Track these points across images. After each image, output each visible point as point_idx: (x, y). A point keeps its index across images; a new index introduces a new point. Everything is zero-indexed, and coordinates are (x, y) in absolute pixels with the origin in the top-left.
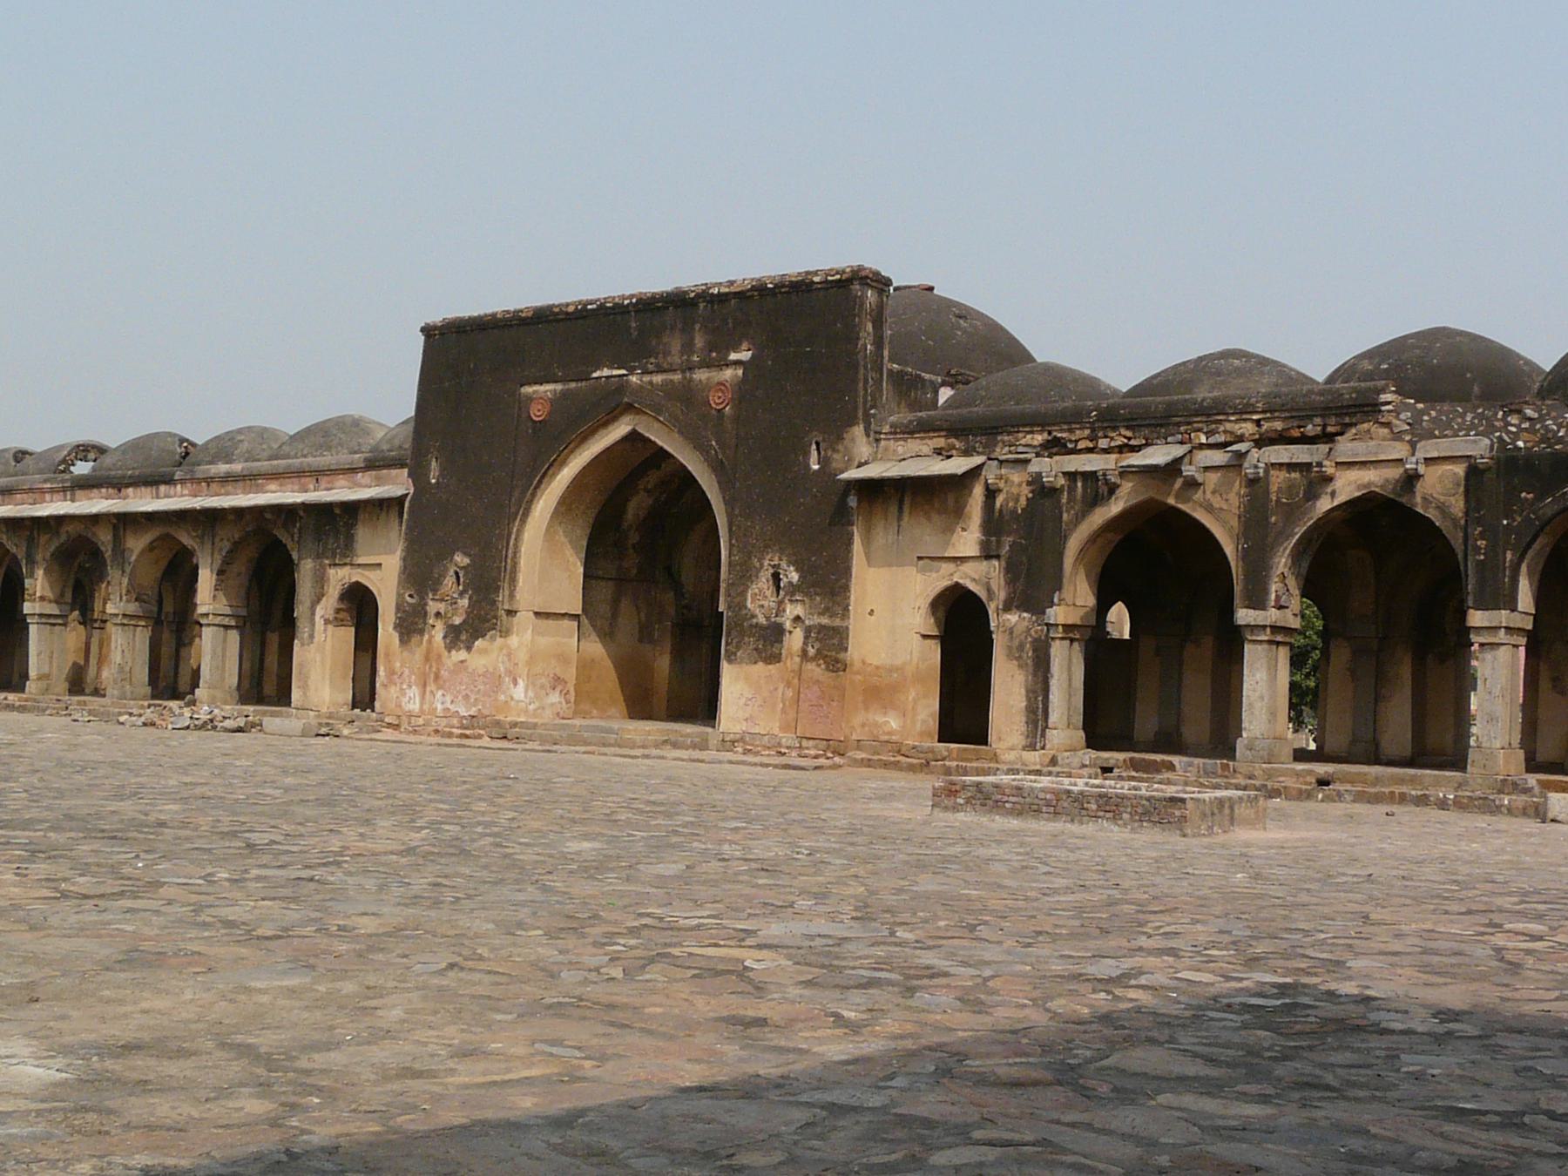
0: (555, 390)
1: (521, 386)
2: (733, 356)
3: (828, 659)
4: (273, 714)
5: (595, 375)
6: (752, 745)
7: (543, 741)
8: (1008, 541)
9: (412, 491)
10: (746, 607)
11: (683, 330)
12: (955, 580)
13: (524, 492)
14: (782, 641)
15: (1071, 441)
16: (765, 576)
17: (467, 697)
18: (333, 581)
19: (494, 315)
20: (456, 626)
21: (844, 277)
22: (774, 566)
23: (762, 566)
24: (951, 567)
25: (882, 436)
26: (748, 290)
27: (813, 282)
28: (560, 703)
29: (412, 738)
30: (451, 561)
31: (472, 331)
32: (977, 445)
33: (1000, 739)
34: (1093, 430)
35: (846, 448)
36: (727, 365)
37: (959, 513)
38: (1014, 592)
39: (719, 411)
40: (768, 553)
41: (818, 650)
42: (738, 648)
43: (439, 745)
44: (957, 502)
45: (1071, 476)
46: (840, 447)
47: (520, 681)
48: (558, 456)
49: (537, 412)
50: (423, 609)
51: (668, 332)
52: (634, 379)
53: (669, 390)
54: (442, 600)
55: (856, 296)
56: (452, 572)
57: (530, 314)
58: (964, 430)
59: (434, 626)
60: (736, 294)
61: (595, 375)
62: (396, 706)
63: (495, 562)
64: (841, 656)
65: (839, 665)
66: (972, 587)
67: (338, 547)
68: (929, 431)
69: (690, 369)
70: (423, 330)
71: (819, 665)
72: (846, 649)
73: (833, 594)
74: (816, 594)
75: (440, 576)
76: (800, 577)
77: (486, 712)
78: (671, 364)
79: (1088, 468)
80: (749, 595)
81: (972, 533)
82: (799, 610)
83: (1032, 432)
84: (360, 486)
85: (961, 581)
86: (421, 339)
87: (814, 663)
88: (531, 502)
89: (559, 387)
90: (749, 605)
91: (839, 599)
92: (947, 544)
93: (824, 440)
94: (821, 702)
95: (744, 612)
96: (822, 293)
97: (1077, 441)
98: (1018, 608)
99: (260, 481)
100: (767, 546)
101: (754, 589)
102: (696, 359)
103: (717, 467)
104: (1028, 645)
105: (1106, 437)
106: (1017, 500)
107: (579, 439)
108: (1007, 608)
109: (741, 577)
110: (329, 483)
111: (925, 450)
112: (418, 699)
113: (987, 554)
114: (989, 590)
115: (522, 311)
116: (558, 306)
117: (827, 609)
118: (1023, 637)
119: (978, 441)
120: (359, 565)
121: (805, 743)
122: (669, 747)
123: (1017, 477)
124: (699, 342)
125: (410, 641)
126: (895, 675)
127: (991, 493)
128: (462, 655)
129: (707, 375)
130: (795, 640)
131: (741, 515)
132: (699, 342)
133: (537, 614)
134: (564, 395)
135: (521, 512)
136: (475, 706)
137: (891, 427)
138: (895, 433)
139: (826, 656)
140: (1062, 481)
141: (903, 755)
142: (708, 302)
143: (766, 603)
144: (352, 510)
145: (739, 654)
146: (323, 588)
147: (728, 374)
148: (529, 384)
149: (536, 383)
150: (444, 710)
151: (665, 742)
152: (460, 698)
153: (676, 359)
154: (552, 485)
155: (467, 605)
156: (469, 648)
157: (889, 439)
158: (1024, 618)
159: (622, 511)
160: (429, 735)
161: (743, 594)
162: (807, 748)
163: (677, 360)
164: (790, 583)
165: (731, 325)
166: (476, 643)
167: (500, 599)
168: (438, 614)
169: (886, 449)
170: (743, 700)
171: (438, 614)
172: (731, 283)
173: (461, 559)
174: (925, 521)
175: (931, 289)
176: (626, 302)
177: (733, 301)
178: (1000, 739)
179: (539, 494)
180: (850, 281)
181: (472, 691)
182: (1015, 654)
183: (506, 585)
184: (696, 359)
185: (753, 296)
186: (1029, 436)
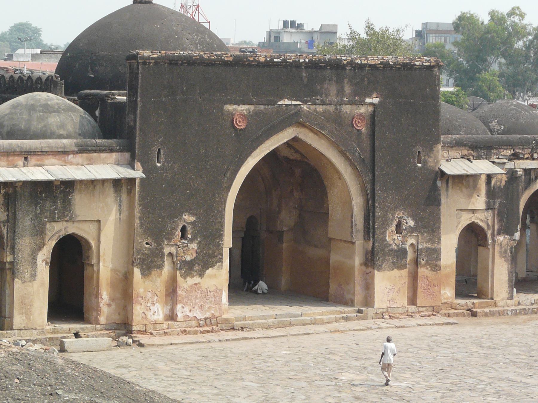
2: (368, 100)
5: (279, 103)
8: (498, 201)
10: (386, 240)
11: (337, 82)
12: (473, 221)
15: (522, 154)
18: (49, 234)
20: (189, 261)
21: (432, 64)
22: (399, 218)
26: (379, 64)
27: (415, 65)
29: (166, 340)
30: (181, 219)
31: (182, 64)
33: (497, 296)
35: (435, 156)
38: (502, 226)
39: (358, 131)
40: (397, 211)
41: (426, 261)
42: (383, 262)
45: (525, 170)
46: (432, 155)
50: (161, 251)
51: (327, 82)
52: (305, 107)
54: (172, 246)
55: (436, 75)
61: (279, 103)
63: (217, 219)
64: (438, 263)
66: (481, 224)
67: (55, 209)
71: (427, 269)
72: (440, 260)
74: (424, 232)
75: (172, 229)
76: (415, 223)
77: (217, 314)
81: (482, 197)
83: (506, 149)
85: (476, 221)
89: (252, 108)
90: (387, 238)
91: (436, 234)
98: (503, 233)
100: (395, 208)
101: (390, 230)
102: (345, 99)
104: (508, 251)
106: (501, 182)
108: (499, 234)
110: (38, 160)
113: (489, 207)
114: (488, 225)
117: (430, 240)
118: (506, 247)
119: (482, 152)
120: (78, 221)
121: (421, 309)
124: (347, 89)
125: (150, 273)
128: (197, 279)
130: (410, 255)
132: (347, 89)
134: (257, 113)
139: (431, 263)
142: (353, 67)
145: (383, 266)
147: (363, 110)
148: (230, 104)
150: (184, 316)
151: (340, 318)
152: (196, 307)
153: (334, 99)
155: (196, 248)
156: (201, 275)
158: (506, 237)
160: (178, 334)
161: (384, 233)
163: (334, 99)
164: (410, 226)
165: (366, 82)
168: (170, 254)
170: (387, 291)
171: (170, 254)
174: (459, 192)
178: (497, 296)
180: (434, 67)
182: (503, 255)
184: (345, 99)
185: (380, 67)
186: (505, 151)
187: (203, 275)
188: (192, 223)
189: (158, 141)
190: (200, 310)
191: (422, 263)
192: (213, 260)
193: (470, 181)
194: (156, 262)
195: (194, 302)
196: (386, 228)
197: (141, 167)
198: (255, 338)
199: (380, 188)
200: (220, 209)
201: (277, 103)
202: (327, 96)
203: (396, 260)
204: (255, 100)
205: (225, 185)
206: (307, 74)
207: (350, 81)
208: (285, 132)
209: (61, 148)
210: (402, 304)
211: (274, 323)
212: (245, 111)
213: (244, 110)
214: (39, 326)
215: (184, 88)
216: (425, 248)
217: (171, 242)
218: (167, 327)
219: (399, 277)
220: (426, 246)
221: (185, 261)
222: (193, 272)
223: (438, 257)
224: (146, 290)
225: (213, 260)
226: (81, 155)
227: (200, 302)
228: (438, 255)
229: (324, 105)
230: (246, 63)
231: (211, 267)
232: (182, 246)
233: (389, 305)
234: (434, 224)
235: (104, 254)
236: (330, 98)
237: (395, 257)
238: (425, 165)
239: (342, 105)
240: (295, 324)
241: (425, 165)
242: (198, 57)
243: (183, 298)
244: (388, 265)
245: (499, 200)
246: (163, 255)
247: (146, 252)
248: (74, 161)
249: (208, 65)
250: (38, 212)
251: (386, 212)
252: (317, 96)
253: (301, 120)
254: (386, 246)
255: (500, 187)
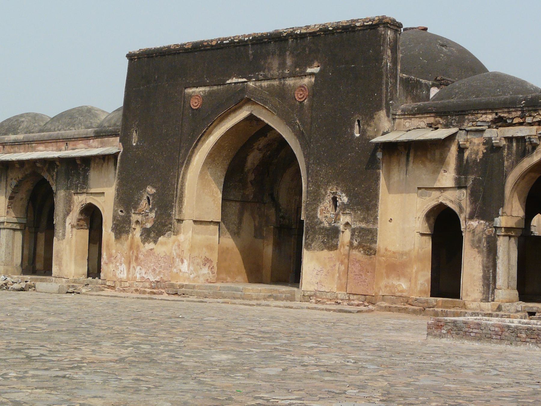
0: (205, 91)
1: (186, 88)
2: (309, 70)
3: (365, 248)
4: (41, 281)
5: (228, 82)
6: (321, 298)
7: (199, 296)
8: (471, 178)
9: (122, 150)
10: (317, 217)
11: (280, 56)
12: (440, 201)
13: (187, 151)
14: (338, 238)
15: (509, 119)
16: (328, 200)
17: (154, 270)
19: (169, 47)
21: (374, 23)
23: (326, 193)
24: (437, 193)
25: (397, 117)
26: (318, 31)
27: (356, 26)
28: (208, 273)
29: (122, 294)
32: (453, 121)
33: (467, 295)
34: (523, 112)
35: (375, 124)
36: (306, 76)
37: (442, 162)
38: (476, 208)
39: (301, 102)
40: (329, 186)
41: (359, 242)
43: (138, 298)
44: (441, 154)
45: (510, 139)
46: (372, 123)
47: (185, 261)
48: (207, 129)
49: (195, 104)
51: (271, 56)
52: (251, 84)
53: (271, 90)
54: (139, 214)
55: (381, 34)
56: (145, 198)
57: (190, 47)
58: (445, 112)
59: (135, 229)
60: (310, 34)
61: (228, 82)
62: (113, 275)
64: (373, 246)
65: (372, 251)
67: (79, 183)
68: (425, 113)
69: (284, 78)
70: (126, 57)
71: (360, 251)
72: (376, 242)
73: (368, 209)
74: (358, 209)
75: (138, 199)
77: (165, 279)
78: (273, 75)
79: (520, 134)
80: (319, 211)
82: (348, 219)
84: (91, 147)
85: (444, 202)
86: (126, 61)
87: (357, 250)
88: (191, 157)
89: (207, 89)
91: (372, 212)
92: (435, 180)
93: (362, 119)
94: (361, 273)
95: (316, 220)
96: (361, 33)
97: (513, 119)
98: (478, 217)
99: (34, 145)
100: (328, 182)
101: (321, 207)
102: (287, 72)
103: (300, 136)
104: (484, 240)
105: (530, 116)
106: (477, 154)
107: (219, 119)
108: (471, 217)
109: (314, 200)
110: (73, 145)
111: (423, 124)
112: (125, 272)
113: (459, 185)
114: (461, 208)
115: (185, 45)
116: (206, 42)
117: (364, 218)
118: (480, 235)
120: (91, 193)
121: (352, 297)
122: (272, 299)
123: (477, 140)
124: (289, 62)
126: (405, 257)
127: (461, 150)
128: (151, 245)
129: (293, 81)
130: (346, 237)
131: (313, 164)
132: (289, 62)
133: (195, 222)
134: (210, 93)
135: (185, 162)
136: (159, 276)
137: (402, 111)
138: (404, 115)
139: (364, 246)
140: (504, 142)
141: (410, 304)
142: (294, 39)
143: (328, 215)
144: (87, 161)
145: (313, 245)
146: (70, 206)
147: (306, 81)
149: (194, 87)
150: (141, 277)
151: (270, 296)
152: (150, 271)
153: (275, 72)
154: (203, 146)
156: (155, 242)
157: (401, 118)
158: (481, 223)
159: (244, 161)
160: (132, 292)
161: (315, 210)
162: (353, 300)
164: (343, 203)
166: (160, 239)
167: (174, 213)
168: (137, 222)
169: (399, 124)
170: (315, 272)
172: (308, 27)
173: (151, 190)
174: (422, 166)
175: (425, 29)
176: (246, 39)
177: (309, 38)
178: (467, 295)
179: (196, 151)
180: (377, 25)
181: (157, 267)
182: (476, 245)
183: (177, 205)
185: (320, 35)
186: (484, 116)
187: (157, 241)
188: (153, 195)
189: (135, 124)
190: (153, 273)
191: (355, 244)
192: (165, 229)
193: (436, 154)
194: (125, 227)
195: (149, 265)
196: (318, 204)
197: (122, 147)
198: (158, 300)
199: (313, 161)
200: (173, 183)
201: (226, 82)
202: (269, 71)
203: (327, 240)
204: (208, 81)
205: (180, 161)
206: (253, 51)
207: (292, 53)
208: (242, 110)
209: (85, 135)
210: (330, 289)
211: (209, 293)
212: (201, 93)
213: (200, 91)
214: (66, 276)
215: (156, 77)
216: (358, 228)
217: (136, 211)
218: (129, 285)
219: (328, 258)
220: (360, 225)
221: (145, 228)
222: (150, 239)
223: (373, 239)
224: (117, 251)
225: (165, 229)
226: (97, 139)
227: (153, 266)
228: (373, 237)
229: (268, 79)
230: (202, 48)
231: (162, 235)
232: (145, 215)
233: (316, 288)
234: (370, 201)
235: (106, 221)
236: (271, 72)
237: (326, 236)
238: (363, 135)
239: (286, 78)
240: (227, 297)
241: (363, 135)
242: (167, 48)
243: (141, 261)
244: (317, 244)
245: (473, 177)
246: (130, 222)
247: (119, 218)
248: (93, 145)
249: (175, 54)
250: (69, 185)
251: (319, 186)
252: (260, 71)
253: (246, 96)
254: (316, 224)
255: (475, 160)
